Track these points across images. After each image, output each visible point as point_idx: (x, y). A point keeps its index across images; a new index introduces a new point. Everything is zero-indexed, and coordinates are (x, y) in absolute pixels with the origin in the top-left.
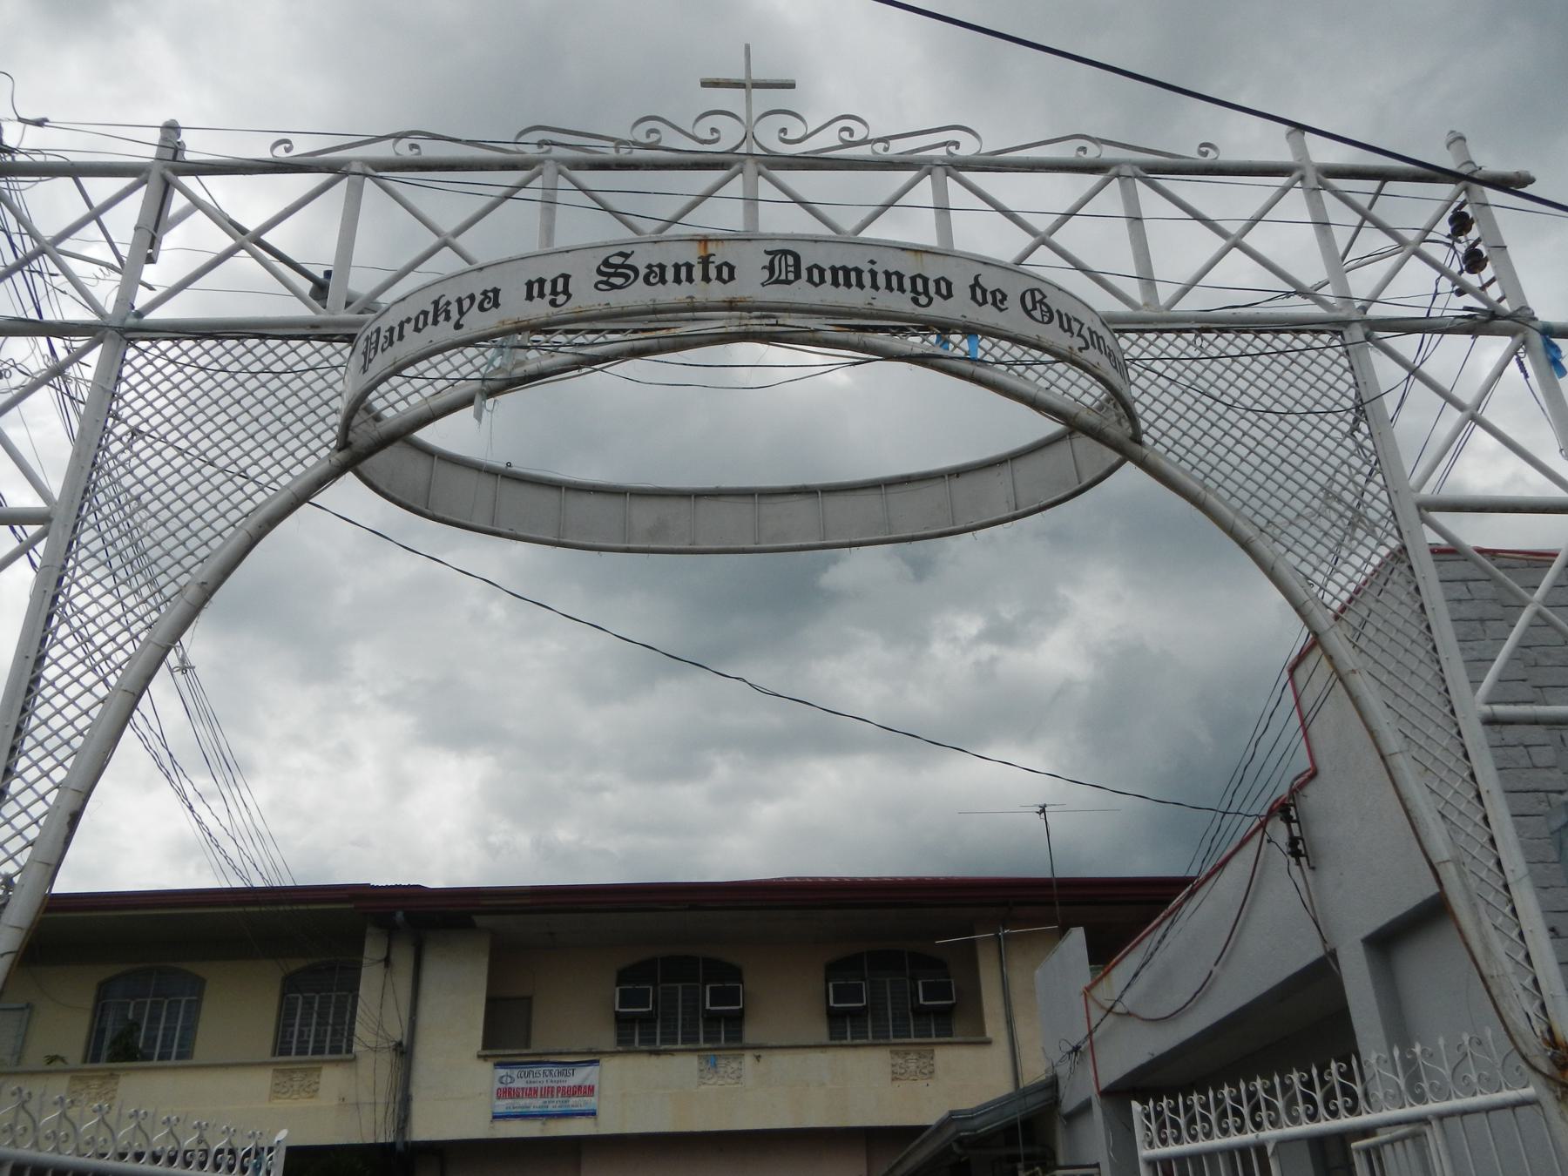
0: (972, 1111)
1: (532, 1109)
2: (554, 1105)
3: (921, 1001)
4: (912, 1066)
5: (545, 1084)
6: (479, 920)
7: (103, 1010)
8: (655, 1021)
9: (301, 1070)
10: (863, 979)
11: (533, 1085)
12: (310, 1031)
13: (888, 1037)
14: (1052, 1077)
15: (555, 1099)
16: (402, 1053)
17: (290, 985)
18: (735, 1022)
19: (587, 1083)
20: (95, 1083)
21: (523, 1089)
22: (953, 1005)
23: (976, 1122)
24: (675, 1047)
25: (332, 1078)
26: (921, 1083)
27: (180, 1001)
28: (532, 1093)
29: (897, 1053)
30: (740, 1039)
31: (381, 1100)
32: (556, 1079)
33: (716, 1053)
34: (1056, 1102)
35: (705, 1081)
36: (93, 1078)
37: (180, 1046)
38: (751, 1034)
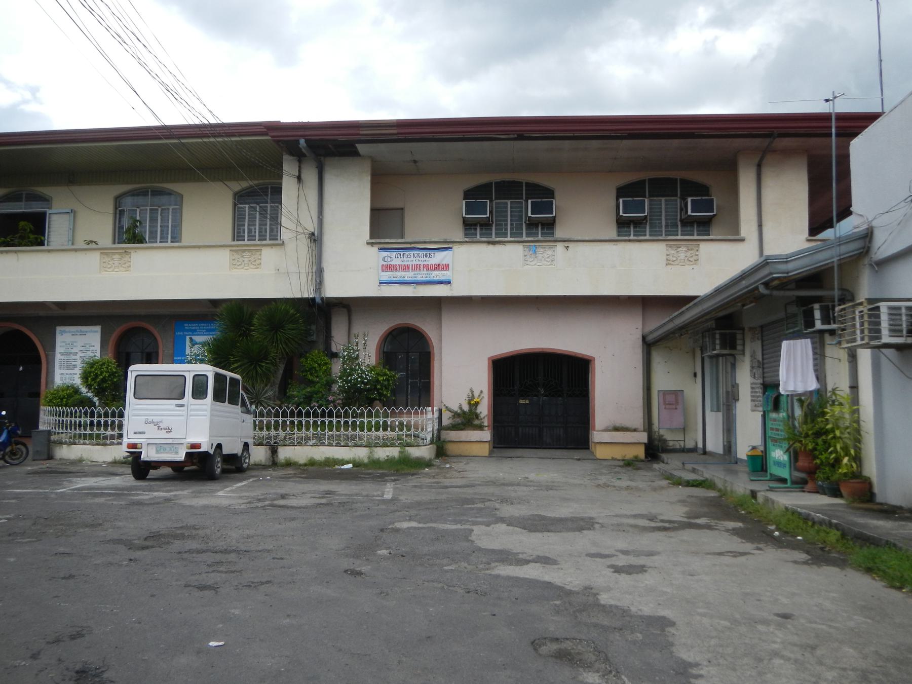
0: (787, 256)
1: (406, 279)
2: (422, 276)
3: (689, 213)
4: (682, 256)
5: (416, 263)
6: (361, 148)
7: (120, 215)
8: (491, 225)
9: (249, 251)
10: (646, 198)
11: (406, 263)
12: (255, 229)
13: (661, 235)
14: (868, 229)
15: (422, 272)
16: (315, 240)
17: (240, 197)
18: (549, 226)
19: (444, 263)
20: (116, 257)
21: (399, 265)
22: (714, 216)
23: (790, 266)
24: (506, 239)
25: (269, 256)
26: (688, 268)
27: (169, 209)
28: (406, 268)
29: (671, 246)
30: (552, 234)
31: (303, 271)
32: (422, 259)
33: (536, 244)
34: (865, 251)
35: (528, 263)
36: (114, 254)
37: (172, 238)
38: (559, 233)
